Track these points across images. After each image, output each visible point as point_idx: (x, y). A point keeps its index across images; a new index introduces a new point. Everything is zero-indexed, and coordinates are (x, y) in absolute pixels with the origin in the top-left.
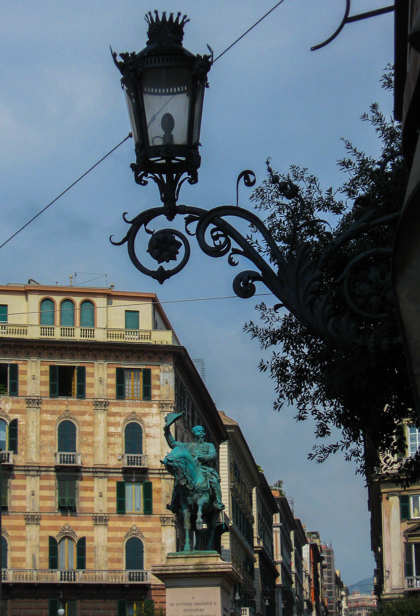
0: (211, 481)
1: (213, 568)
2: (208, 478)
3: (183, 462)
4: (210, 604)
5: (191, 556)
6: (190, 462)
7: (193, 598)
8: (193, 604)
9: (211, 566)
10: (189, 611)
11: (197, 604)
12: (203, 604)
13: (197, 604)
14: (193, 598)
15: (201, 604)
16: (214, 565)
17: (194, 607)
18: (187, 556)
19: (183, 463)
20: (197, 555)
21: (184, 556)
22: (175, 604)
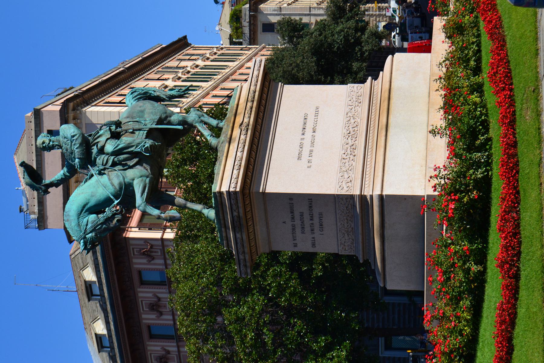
0: (110, 163)
1: (237, 211)
2: (107, 167)
3: (85, 220)
4: (292, 205)
5: (222, 222)
6: (84, 206)
7: (284, 222)
8: (293, 223)
9: (235, 214)
10: (303, 228)
11: (293, 218)
12: (292, 212)
13: (293, 218)
14: (284, 222)
15: (292, 214)
16: (233, 210)
17: (298, 222)
18: (223, 226)
19: (87, 225)
20: (221, 215)
21: (223, 229)
22: (295, 242)
